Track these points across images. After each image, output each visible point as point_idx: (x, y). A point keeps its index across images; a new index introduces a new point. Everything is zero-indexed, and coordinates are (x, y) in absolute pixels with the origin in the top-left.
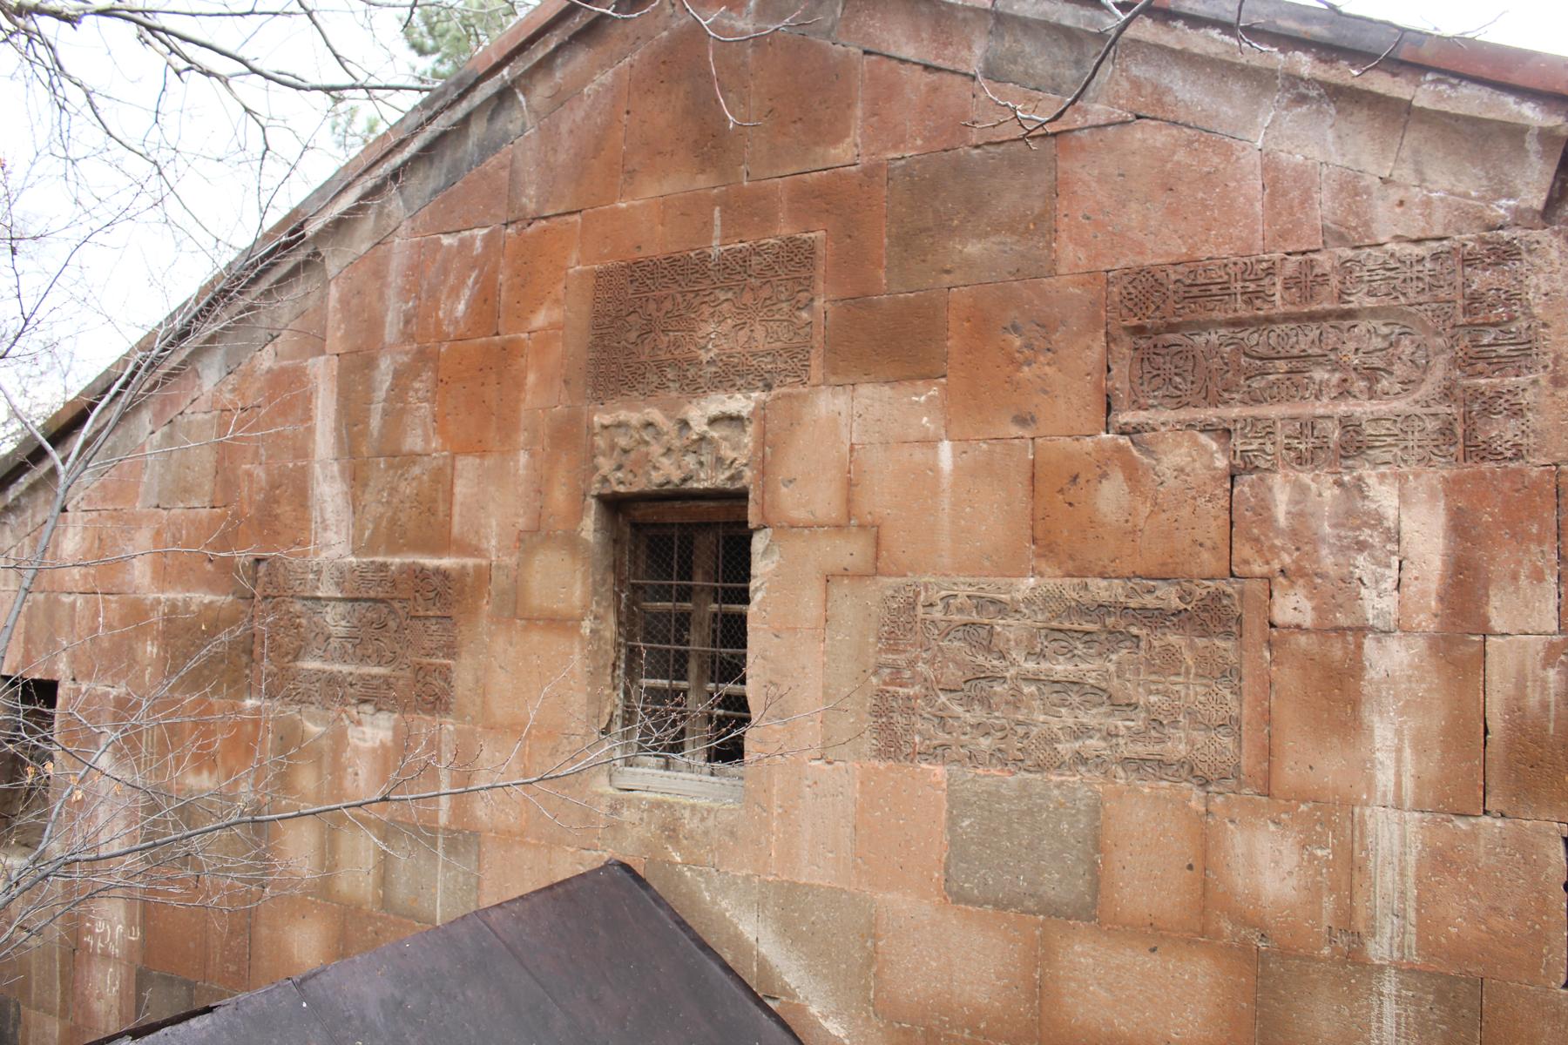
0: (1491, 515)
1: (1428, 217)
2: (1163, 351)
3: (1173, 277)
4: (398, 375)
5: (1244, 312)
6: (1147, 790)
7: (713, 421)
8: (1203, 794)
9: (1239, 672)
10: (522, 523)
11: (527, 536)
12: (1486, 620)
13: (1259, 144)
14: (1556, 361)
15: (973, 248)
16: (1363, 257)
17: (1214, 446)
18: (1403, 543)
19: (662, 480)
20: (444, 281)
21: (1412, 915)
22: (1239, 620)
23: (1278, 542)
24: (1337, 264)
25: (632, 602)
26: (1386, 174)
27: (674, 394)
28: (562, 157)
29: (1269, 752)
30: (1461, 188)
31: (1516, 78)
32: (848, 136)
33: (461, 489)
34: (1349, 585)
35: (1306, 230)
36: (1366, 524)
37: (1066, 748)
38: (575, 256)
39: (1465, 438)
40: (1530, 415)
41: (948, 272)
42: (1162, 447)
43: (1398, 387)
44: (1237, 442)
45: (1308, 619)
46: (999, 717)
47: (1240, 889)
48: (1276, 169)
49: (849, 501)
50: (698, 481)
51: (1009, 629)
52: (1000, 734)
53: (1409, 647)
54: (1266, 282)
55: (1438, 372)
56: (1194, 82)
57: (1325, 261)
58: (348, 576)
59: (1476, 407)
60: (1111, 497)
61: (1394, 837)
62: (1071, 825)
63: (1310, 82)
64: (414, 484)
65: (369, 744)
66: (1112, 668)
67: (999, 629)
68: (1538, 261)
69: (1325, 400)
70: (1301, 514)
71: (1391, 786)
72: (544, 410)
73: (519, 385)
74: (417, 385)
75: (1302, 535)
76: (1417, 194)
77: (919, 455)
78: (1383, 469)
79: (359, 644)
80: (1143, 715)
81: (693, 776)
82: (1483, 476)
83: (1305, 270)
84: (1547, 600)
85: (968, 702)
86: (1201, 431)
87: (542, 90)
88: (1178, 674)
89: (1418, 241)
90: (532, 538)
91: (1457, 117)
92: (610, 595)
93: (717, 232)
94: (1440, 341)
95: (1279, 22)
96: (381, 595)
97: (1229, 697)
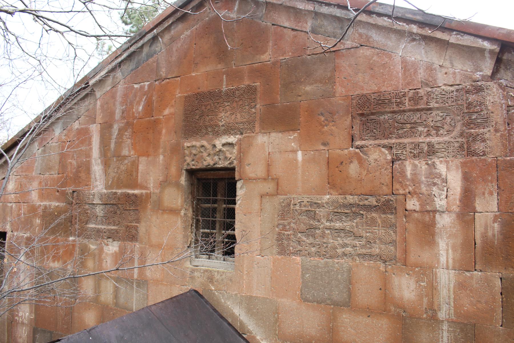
0: (476, 174)
1: (455, 78)
2: (370, 121)
3: (373, 97)
4: (120, 130)
5: (396, 109)
6: (366, 264)
7: (224, 145)
8: (384, 265)
9: (396, 225)
10: (161, 179)
12: (475, 208)
13: (400, 54)
14: (496, 124)
15: (308, 88)
16: (434, 91)
17: (387, 152)
18: (448, 183)
19: (207, 164)
20: (135, 99)
21: (452, 304)
22: (395, 208)
23: (408, 183)
24: (426, 93)
25: (197, 204)
26: (441, 64)
27: (211, 136)
28: (174, 59)
29: (405, 251)
30: (465, 69)
31: (481, 33)
33: (141, 167)
34: (431, 197)
35: (416, 82)
36: (436, 177)
37: (340, 251)
38: (178, 91)
39: (467, 149)
40: (488, 141)
41: (300, 96)
42: (370, 152)
43: (446, 133)
44: (394, 151)
45: (418, 208)
46: (318, 241)
47: (397, 296)
48: (406, 62)
50: (219, 164)
51: (321, 212)
52: (318, 247)
53: (450, 217)
54: (403, 99)
55: (458, 128)
56: (379, 34)
57: (422, 92)
58: (104, 196)
59: (471, 139)
60: (353, 169)
61: (446, 278)
62: (342, 276)
63: (416, 34)
64: (126, 166)
65: (111, 252)
66: (354, 224)
67: (317, 212)
68: (489, 92)
69: (422, 137)
70: (415, 174)
71: (445, 262)
72: (168, 141)
73: (160, 133)
74: (126, 133)
75: (415, 181)
76: (451, 70)
77: (291, 156)
78: (441, 159)
79: (107, 219)
80: (365, 240)
81: (216, 261)
82: (473, 161)
83: (415, 95)
84: (494, 201)
85: (308, 236)
86: (383, 147)
87: (167, 37)
88: (376, 226)
89: (452, 86)
90: (164, 184)
91: (463, 46)
92: (190, 202)
93: (225, 83)
94: (459, 118)
95: (406, 15)
96: (115, 203)
97: (392, 233)
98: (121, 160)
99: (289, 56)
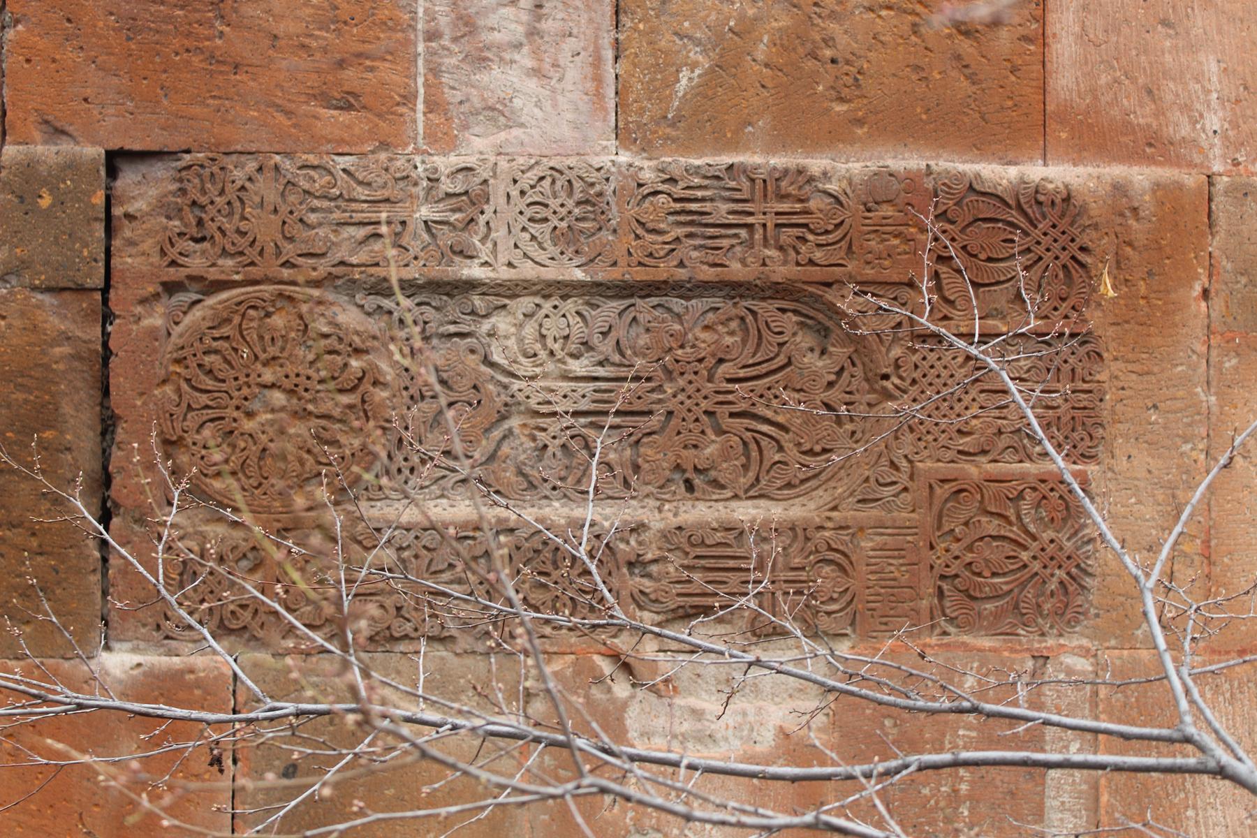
79: (642, 425)
96: (781, 271)
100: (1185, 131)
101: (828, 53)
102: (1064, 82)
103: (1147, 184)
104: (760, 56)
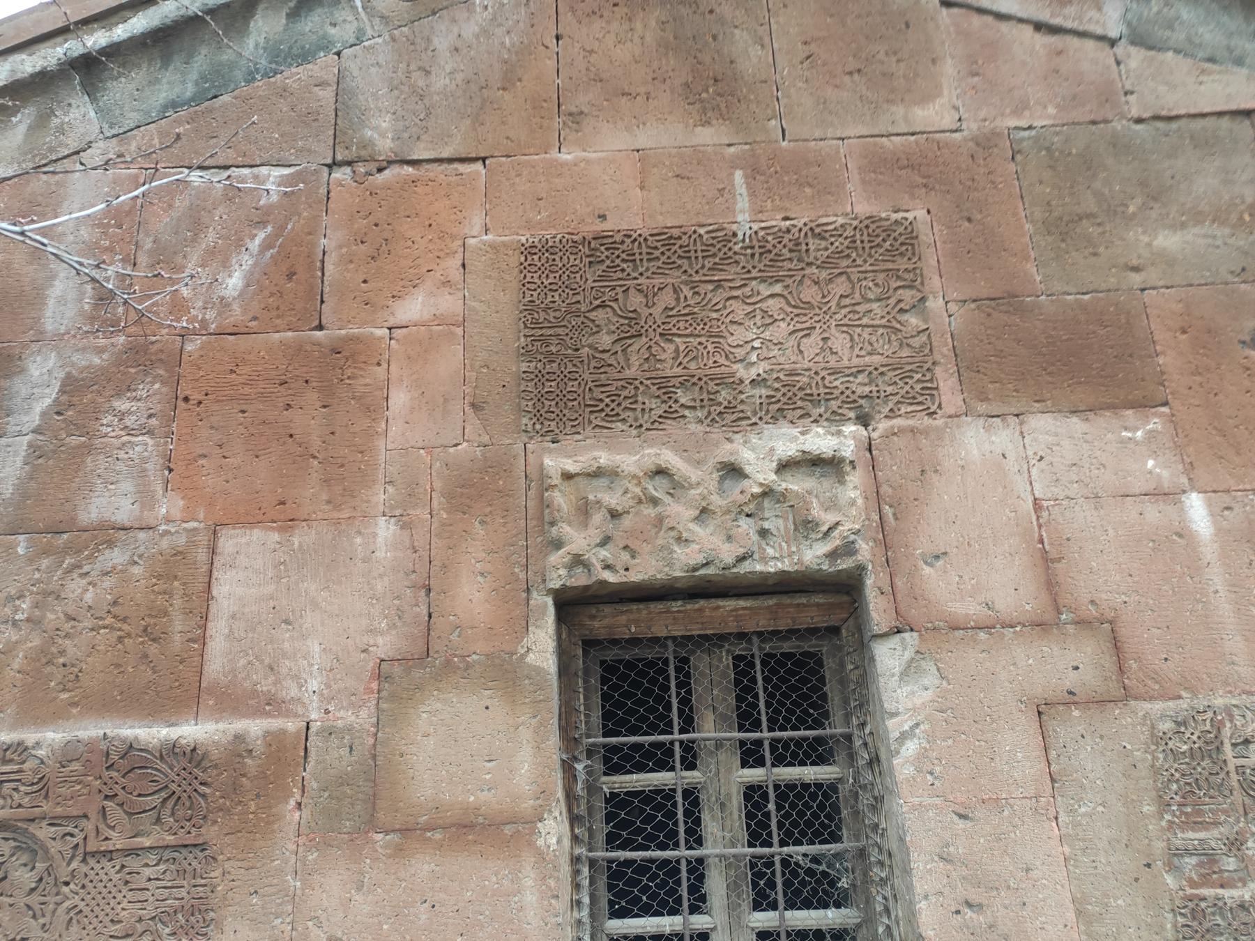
4: (71, 386)
7: (784, 467)
10: (385, 645)
11: (397, 669)
15: (1168, 241)
19: (700, 559)
20: (195, 239)
32: (940, 95)
33: (230, 589)
41: (1136, 269)
49: (1051, 585)
50: (764, 559)
64: (108, 582)
72: (429, 449)
73: (374, 407)
74: (122, 405)
77: (1153, 513)
90: (415, 668)
98: (67, 550)
99: (1049, 117)
100: (294, 692)
101: (61, 660)
102: (213, 667)
103: (260, 733)
104: (16, 666)
